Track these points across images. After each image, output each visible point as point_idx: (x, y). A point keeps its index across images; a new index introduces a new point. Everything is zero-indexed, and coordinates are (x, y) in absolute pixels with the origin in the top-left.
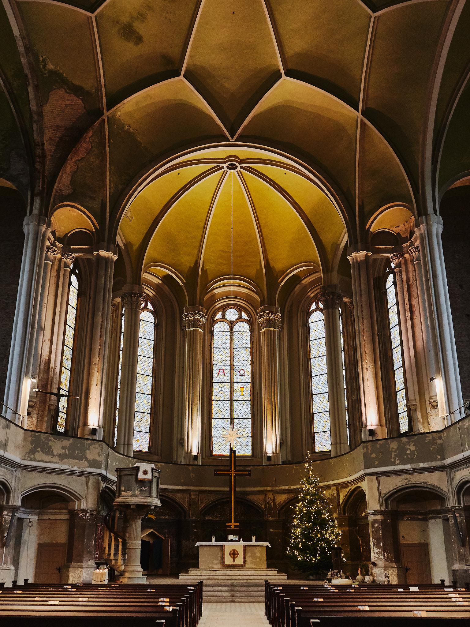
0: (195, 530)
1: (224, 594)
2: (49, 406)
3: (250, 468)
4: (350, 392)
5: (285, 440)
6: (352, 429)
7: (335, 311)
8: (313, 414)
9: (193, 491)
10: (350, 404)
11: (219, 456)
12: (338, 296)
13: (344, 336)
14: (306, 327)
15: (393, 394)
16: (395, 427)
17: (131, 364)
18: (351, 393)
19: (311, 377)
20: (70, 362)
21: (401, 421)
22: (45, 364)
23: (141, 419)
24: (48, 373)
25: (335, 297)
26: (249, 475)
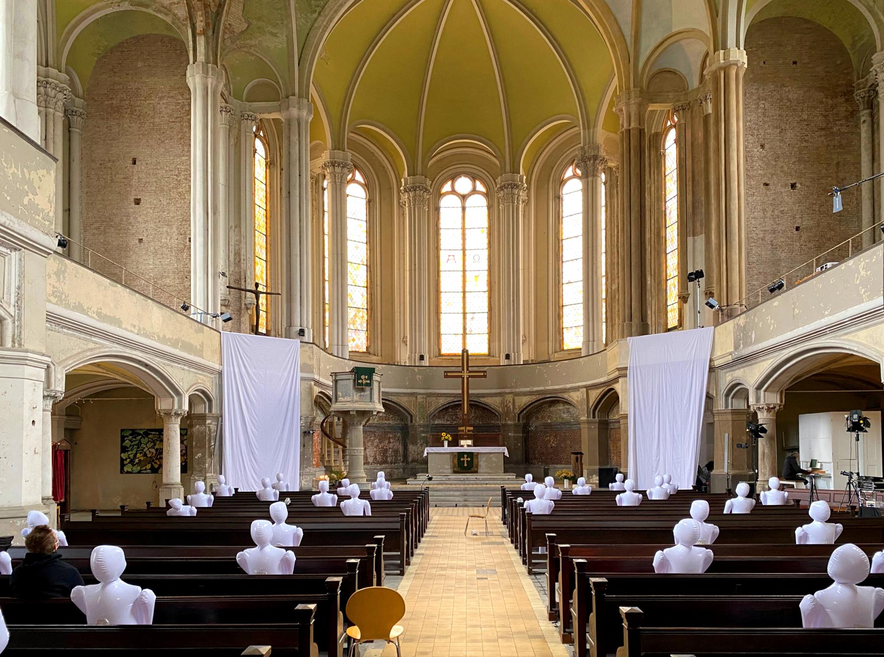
0: (423, 435)
1: (457, 499)
2: (245, 304)
3: (485, 369)
4: (609, 280)
5: (527, 336)
6: (610, 324)
7: (596, 179)
8: (563, 306)
9: (420, 394)
10: (609, 295)
11: (449, 355)
12: (601, 160)
13: (606, 211)
14: (558, 198)
15: (663, 282)
16: (662, 321)
17: (340, 252)
18: (612, 281)
19: (562, 262)
20: (264, 251)
21: (670, 315)
22: (235, 255)
23: (355, 316)
24: (240, 266)
25: (598, 161)
26: (485, 376)
